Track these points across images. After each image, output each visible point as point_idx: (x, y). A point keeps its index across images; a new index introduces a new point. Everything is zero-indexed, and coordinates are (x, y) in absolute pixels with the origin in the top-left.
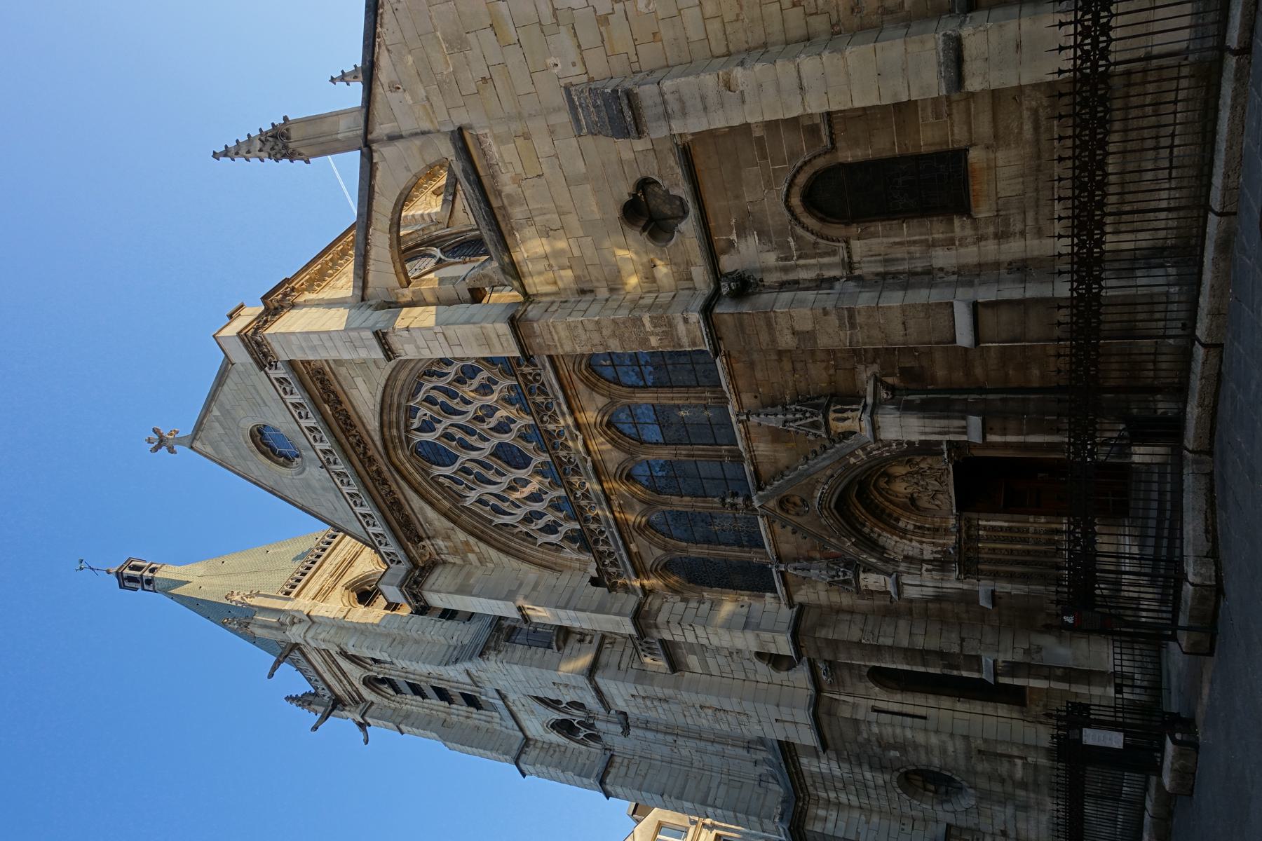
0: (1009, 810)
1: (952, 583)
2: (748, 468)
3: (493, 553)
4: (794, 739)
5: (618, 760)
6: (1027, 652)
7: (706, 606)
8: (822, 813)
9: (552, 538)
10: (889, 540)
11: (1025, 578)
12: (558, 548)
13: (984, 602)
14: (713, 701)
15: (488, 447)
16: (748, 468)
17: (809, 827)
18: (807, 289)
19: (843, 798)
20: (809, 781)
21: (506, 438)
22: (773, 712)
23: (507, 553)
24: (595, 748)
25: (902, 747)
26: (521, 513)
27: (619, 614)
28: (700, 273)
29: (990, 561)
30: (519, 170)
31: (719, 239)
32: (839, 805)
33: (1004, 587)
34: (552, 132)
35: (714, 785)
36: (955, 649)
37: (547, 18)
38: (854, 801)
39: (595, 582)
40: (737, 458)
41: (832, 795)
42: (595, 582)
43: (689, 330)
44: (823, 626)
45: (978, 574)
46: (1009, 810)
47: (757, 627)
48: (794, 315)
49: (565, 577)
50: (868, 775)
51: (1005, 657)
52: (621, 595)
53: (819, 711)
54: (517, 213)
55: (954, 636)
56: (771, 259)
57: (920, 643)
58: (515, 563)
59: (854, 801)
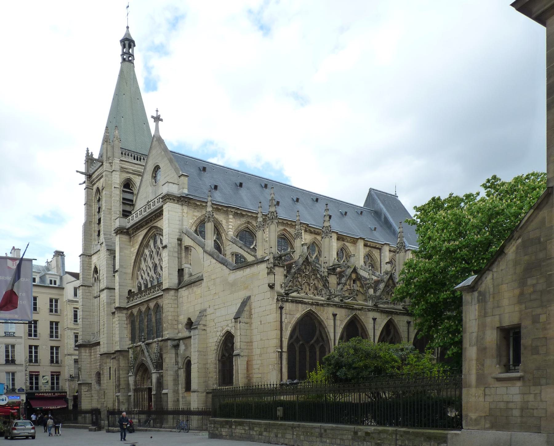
0: (97, 398)
1: (132, 387)
2: (151, 341)
3: (134, 257)
4: (102, 346)
5: (90, 288)
6: (123, 402)
7: (125, 326)
8: (87, 351)
9: (140, 278)
10: (140, 374)
11: (134, 402)
12: (138, 279)
13: (130, 394)
14: (106, 325)
15: (157, 262)
16: (151, 341)
17: (82, 349)
18: (176, 360)
19: (92, 357)
20: (95, 348)
21: (159, 269)
22: (106, 342)
23: (135, 262)
24: (92, 280)
25: (103, 374)
26: (145, 269)
27: (120, 302)
28: (180, 335)
29: (137, 395)
30: (197, 293)
31: (184, 341)
32: (91, 355)
33: (132, 398)
34: (201, 303)
35: (89, 320)
36: (121, 387)
37: (216, 307)
38: (92, 360)
39: (130, 291)
40: (153, 339)
41: (93, 354)
42: (130, 291)
43: (167, 334)
44: (123, 357)
45: (134, 392)
46: (97, 398)
47: (120, 341)
48: (169, 359)
49: (130, 282)
50: (98, 364)
51: (121, 398)
52: (126, 301)
53: (107, 355)
54: (190, 290)
55: (124, 387)
56: (182, 352)
57: (122, 380)
58: (132, 264)
59: (92, 360)
